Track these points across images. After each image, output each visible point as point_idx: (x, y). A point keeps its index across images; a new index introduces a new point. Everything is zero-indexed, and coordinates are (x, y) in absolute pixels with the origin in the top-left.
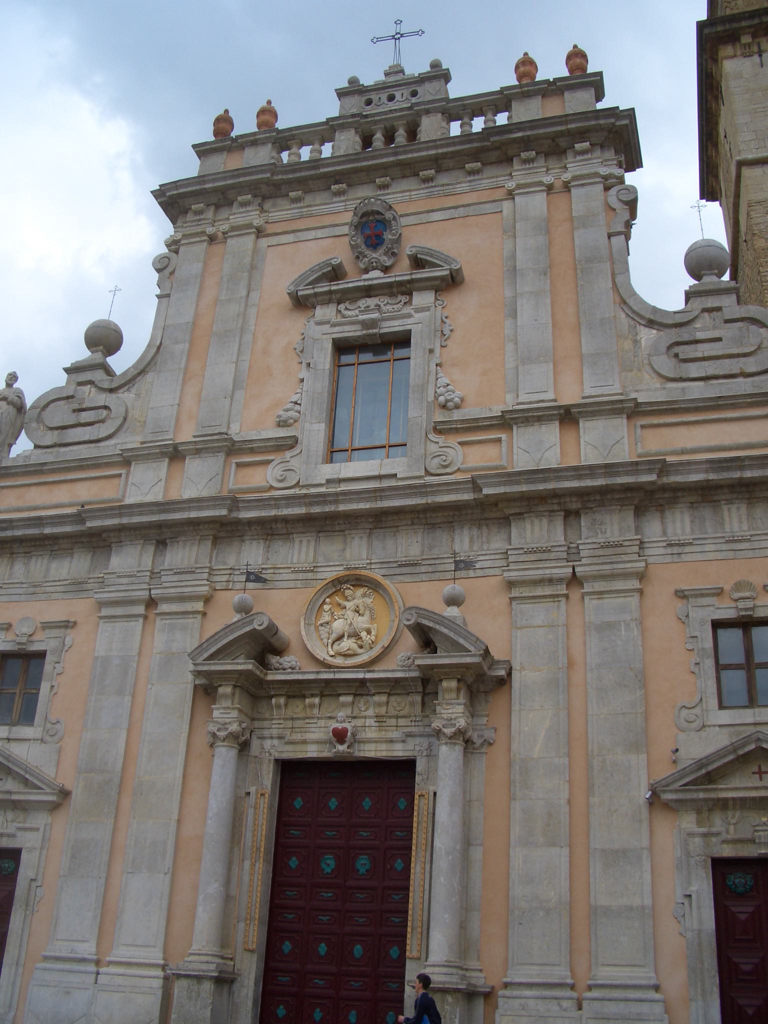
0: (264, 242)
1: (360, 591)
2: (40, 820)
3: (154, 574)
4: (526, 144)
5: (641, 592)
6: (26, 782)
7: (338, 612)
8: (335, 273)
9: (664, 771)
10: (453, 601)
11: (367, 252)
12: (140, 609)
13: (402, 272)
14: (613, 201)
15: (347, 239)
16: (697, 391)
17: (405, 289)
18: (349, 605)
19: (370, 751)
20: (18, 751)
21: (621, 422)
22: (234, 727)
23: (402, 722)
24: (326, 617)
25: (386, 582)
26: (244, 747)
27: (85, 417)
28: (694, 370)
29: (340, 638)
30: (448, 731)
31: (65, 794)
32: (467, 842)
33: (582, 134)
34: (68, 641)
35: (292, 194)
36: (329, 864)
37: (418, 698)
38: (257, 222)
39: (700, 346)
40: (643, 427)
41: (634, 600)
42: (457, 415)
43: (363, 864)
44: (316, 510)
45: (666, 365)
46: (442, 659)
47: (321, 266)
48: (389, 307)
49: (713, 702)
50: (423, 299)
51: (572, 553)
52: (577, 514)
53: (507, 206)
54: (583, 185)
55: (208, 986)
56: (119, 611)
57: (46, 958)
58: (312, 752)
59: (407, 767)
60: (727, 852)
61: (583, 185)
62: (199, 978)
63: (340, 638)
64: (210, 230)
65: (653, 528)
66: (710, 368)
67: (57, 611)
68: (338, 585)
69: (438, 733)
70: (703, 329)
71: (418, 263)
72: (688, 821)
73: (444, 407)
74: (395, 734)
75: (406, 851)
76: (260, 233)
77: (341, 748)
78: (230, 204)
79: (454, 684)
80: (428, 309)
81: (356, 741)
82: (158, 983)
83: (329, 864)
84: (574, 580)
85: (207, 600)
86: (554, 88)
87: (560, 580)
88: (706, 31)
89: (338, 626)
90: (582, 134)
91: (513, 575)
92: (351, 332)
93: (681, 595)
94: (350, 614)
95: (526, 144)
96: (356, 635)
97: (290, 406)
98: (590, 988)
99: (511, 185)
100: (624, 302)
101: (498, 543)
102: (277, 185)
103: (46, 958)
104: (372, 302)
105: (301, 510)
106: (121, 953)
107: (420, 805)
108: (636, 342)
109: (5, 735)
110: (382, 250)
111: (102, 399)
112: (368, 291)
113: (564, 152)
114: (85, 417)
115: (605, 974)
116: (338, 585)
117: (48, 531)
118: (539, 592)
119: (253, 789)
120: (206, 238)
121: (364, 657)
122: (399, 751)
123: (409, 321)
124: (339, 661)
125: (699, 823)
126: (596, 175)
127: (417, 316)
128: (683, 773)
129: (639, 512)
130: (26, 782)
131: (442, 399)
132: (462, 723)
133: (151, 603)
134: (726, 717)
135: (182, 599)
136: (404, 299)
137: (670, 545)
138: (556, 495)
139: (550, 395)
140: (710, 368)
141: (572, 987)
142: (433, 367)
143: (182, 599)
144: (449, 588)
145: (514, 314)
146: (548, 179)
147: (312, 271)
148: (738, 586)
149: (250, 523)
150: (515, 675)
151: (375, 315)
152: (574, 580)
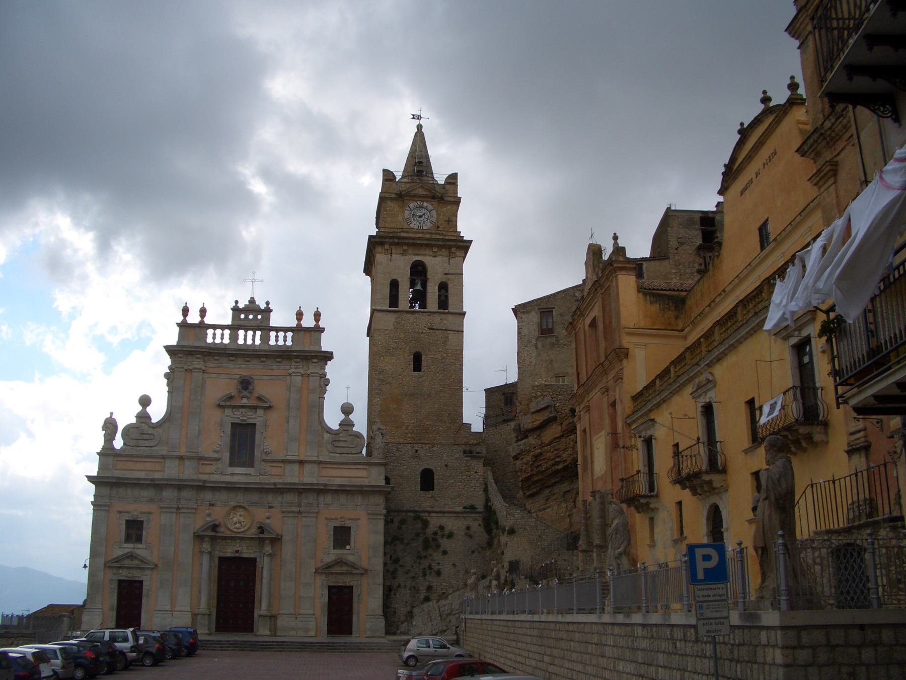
0: (206, 375)
1: (241, 510)
2: (148, 572)
3: (179, 499)
4: (297, 357)
5: (316, 517)
6: (142, 561)
7: (235, 516)
8: (231, 398)
9: (319, 565)
10: (268, 518)
11: (243, 391)
12: (175, 510)
13: (253, 402)
14: (322, 383)
15: (236, 381)
16: (338, 458)
17: (255, 408)
18: (238, 514)
19: (245, 555)
20: (138, 552)
21: (316, 466)
22: (209, 550)
23: (253, 548)
24: (231, 517)
25: (248, 508)
26: (210, 553)
27: (145, 437)
28: (338, 450)
29: (236, 523)
30: (267, 553)
31: (156, 565)
32: (270, 580)
33: (315, 357)
34: (150, 518)
35: (216, 357)
36: (232, 584)
37: (258, 542)
38: (204, 368)
39: (341, 443)
40: (322, 468)
41: (314, 519)
42: (269, 457)
43: (242, 584)
44: (229, 486)
45: (330, 447)
46: (265, 535)
47: (227, 395)
48: (249, 413)
49: (332, 548)
50: (260, 412)
51: (300, 505)
52: (302, 493)
53: (288, 378)
54: (313, 376)
55: (207, 616)
56: (167, 510)
57: (155, 611)
58: (229, 555)
59: (254, 561)
60: (332, 584)
61: (313, 376)
62: (204, 615)
63: (236, 523)
64: (186, 367)
65: (321, 498)
66: (342, 450)
67: (146, 508)
68: (235, 508)
69: (264, 554)
70: (342, 437)
71: (259, 398)
72: (323, 577)
73: (266, 453)
74: (251, 551)
75: (254, 581)
76: (204, 371)
77: (237, 555)
78: (192, 355)
79: (269, 542)
80: (261, 417)
81: (241, 553)
82: (190, 616)
83: (232, 584)
84: (300, 512)
85: (196, 509)
86: (308, 330)
87: (295, 512)
88: (372, 240)
89: (235, 519)
90: (315, 357)
91: (284, 510)
92: (237, 421)
93: (327, 519)
94: (238, 516)
95: (297, 357)
96: (240, 523)
97: (218, 446)
98: (299, 615)
99: (291, 372)
100: (321, 423)
101: (280, 499)
102: (210, 353)
103: (155, 611)
104: (244, 410)
105: (225, 485)
106: (177, 609)
107: (258, 571)
108: (323, 438)
109: (133, 547)
110: (248, 391)
111: (151, 431)
112: (243, 407)
113: (309, 359)
114: (145, 437)
115: (302, 612)
116: (235, 508)
117: (141, 482)
118: (290, 515)
119: (213, 565)
120: (183, 370)
121: (243, 530)
122: (252, 556)
123: (256, 420)
124: (235, 530)
125: (326, 577)
126: (318, 373)
127: (259, 418)
128: (323, 566)
129: (318, 494)
130: (142, 561)
131: (265, 451)
132: (270, 551)
133: (178, 508)
134: (335, 551)
135: (188, 508)
136: (254, 411)
137: (325, 504)
138: (297, 488)
139: (297, 454)
140: (342, 450)
141: (295, 614)
142: (263, 439)
143: (188, 508)
144: (267, 514)
145: (288, 422)
146: (303, 372)
147: (224, 396)
148: (341, 518)
149: (208, 486)
150: (283, 538)
151: (246, 418)
152: (300, 512)
